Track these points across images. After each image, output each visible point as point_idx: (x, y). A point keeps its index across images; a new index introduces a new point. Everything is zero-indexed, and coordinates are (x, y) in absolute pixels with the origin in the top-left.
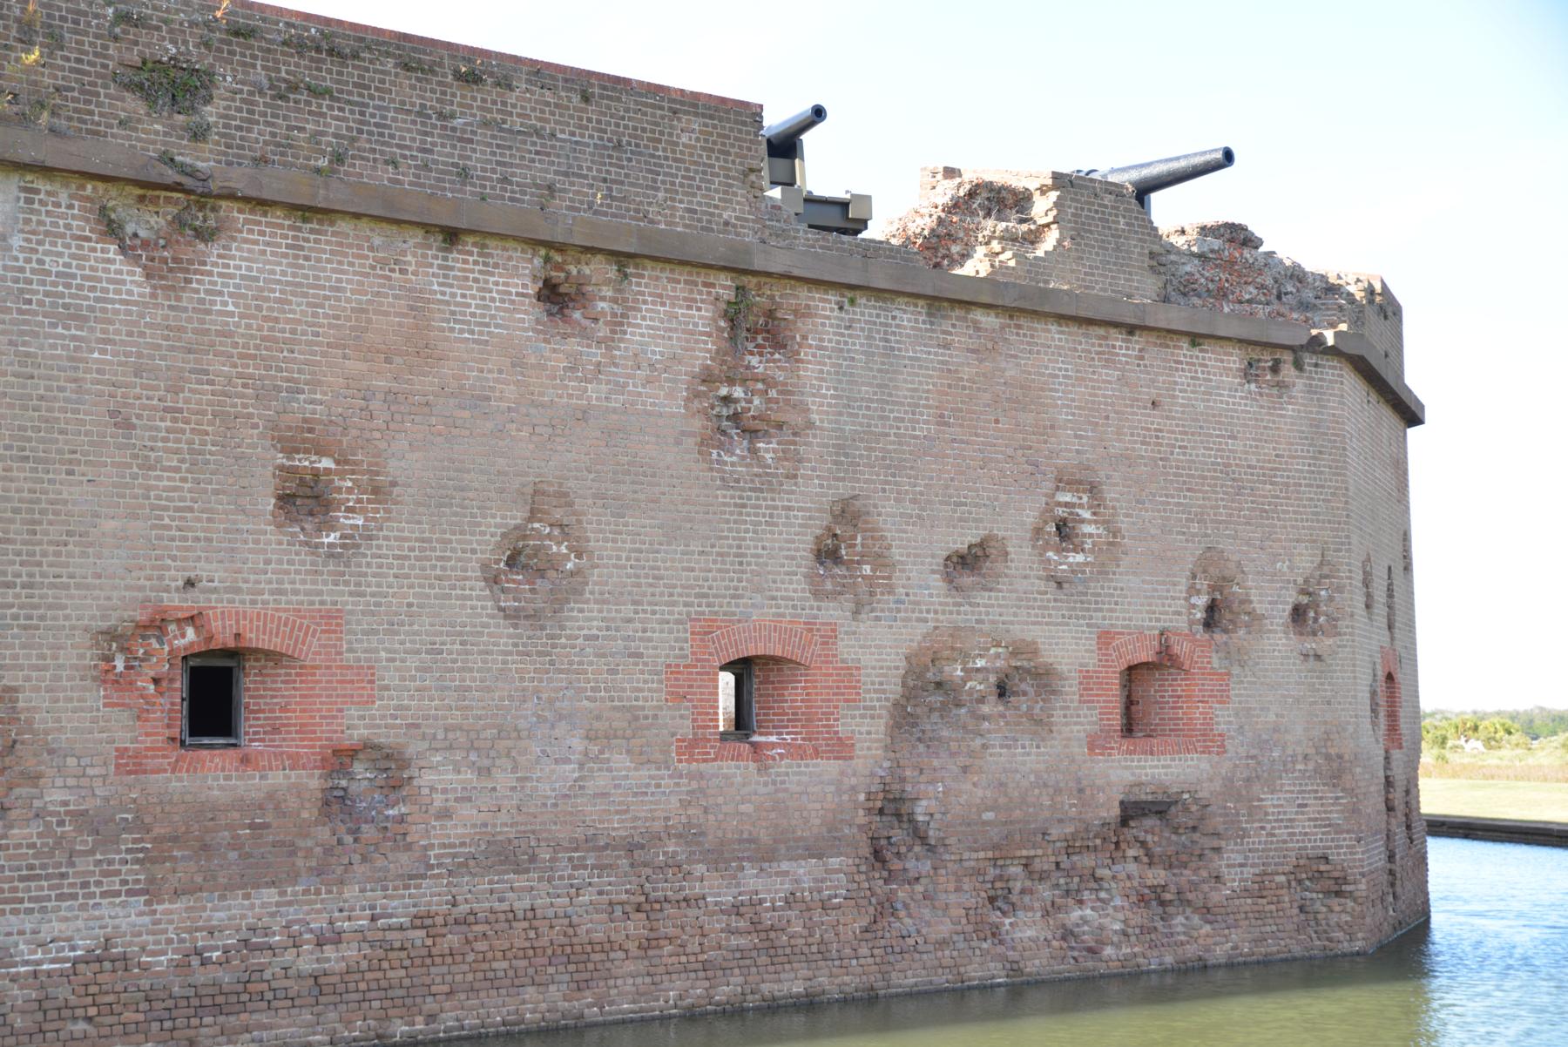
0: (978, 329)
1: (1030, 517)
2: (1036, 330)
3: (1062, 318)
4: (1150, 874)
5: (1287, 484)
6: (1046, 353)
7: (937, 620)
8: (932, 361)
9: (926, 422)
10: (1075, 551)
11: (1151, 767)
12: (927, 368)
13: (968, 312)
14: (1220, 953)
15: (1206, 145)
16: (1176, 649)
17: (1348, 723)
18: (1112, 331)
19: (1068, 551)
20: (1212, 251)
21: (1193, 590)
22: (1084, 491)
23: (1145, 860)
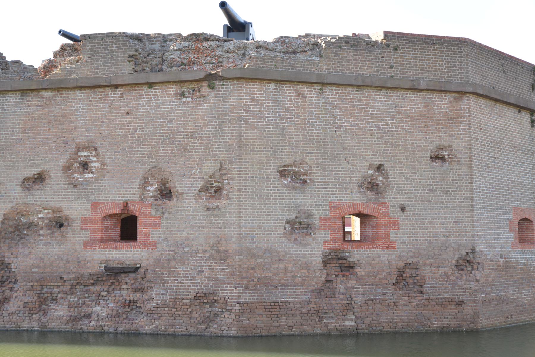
0: (43, 98)
1: (63, 161)
2: (70, 94)
3: (81, 88)
5: (201, 138)
7: (17, 201)
8: (22, 112)
9: (17, 133)
10: (89, 173)
11: (115, 254)
12: (20, 115)
13: (39, 92)
14: (148, 329)
17: (232, 237)
18: (107, 89)
19: (87, 173)
20: (184, 47)
22: (92, 150)
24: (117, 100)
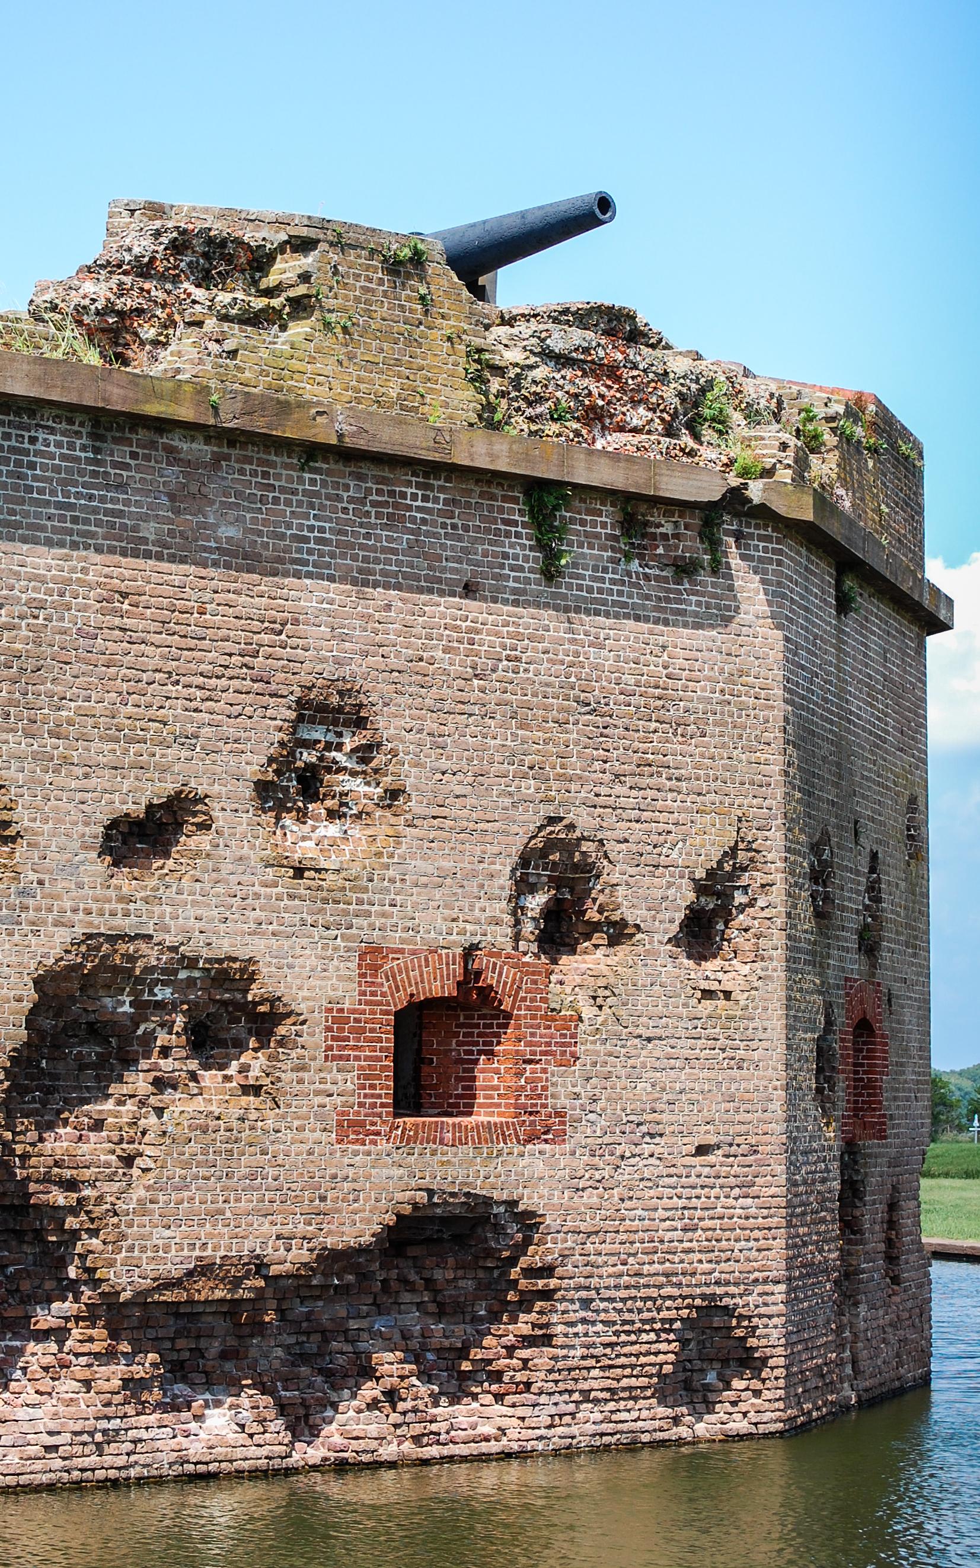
1: (254, 764)
2: (272, 465)
4: (437, 1328)
6: (288, 503)
7: (90, 924)
8: (95, 511)
12: (86, 521)
16: (490, 979)
21: (523, 886)
23: (432, 1308)
24: (434, 524)
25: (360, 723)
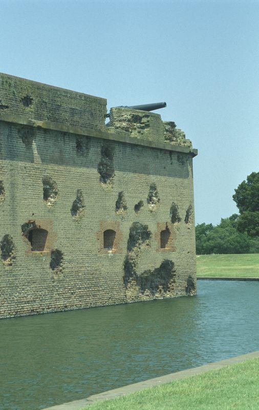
15: (162, 101)
25: (155, 189)
